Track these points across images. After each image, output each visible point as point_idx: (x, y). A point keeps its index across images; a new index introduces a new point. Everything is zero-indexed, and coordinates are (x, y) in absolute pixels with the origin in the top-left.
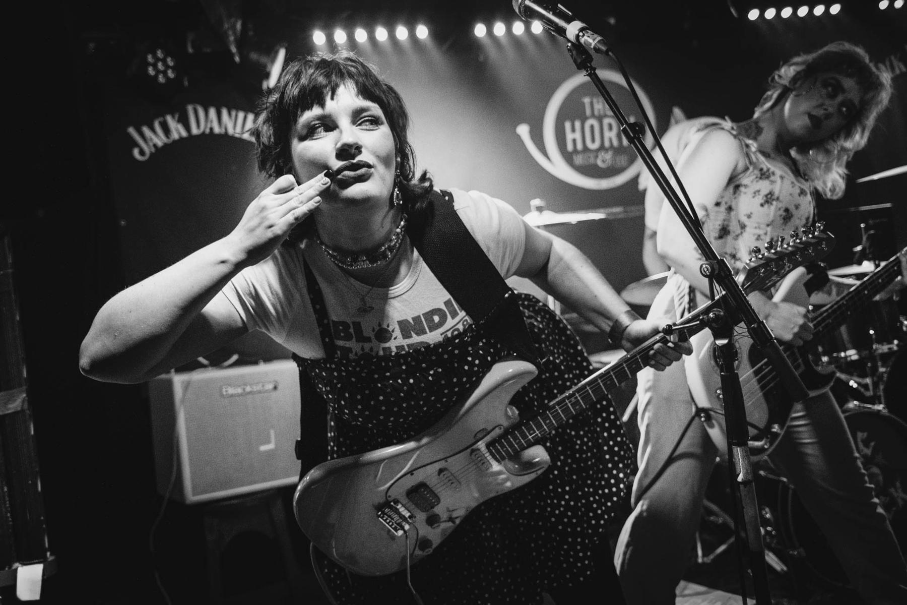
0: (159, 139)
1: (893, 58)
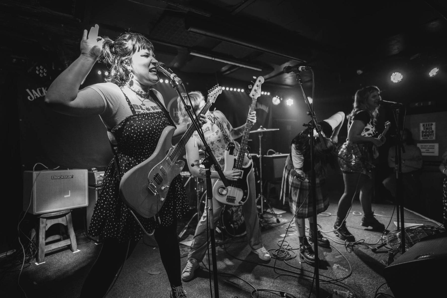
0: (38, 95)
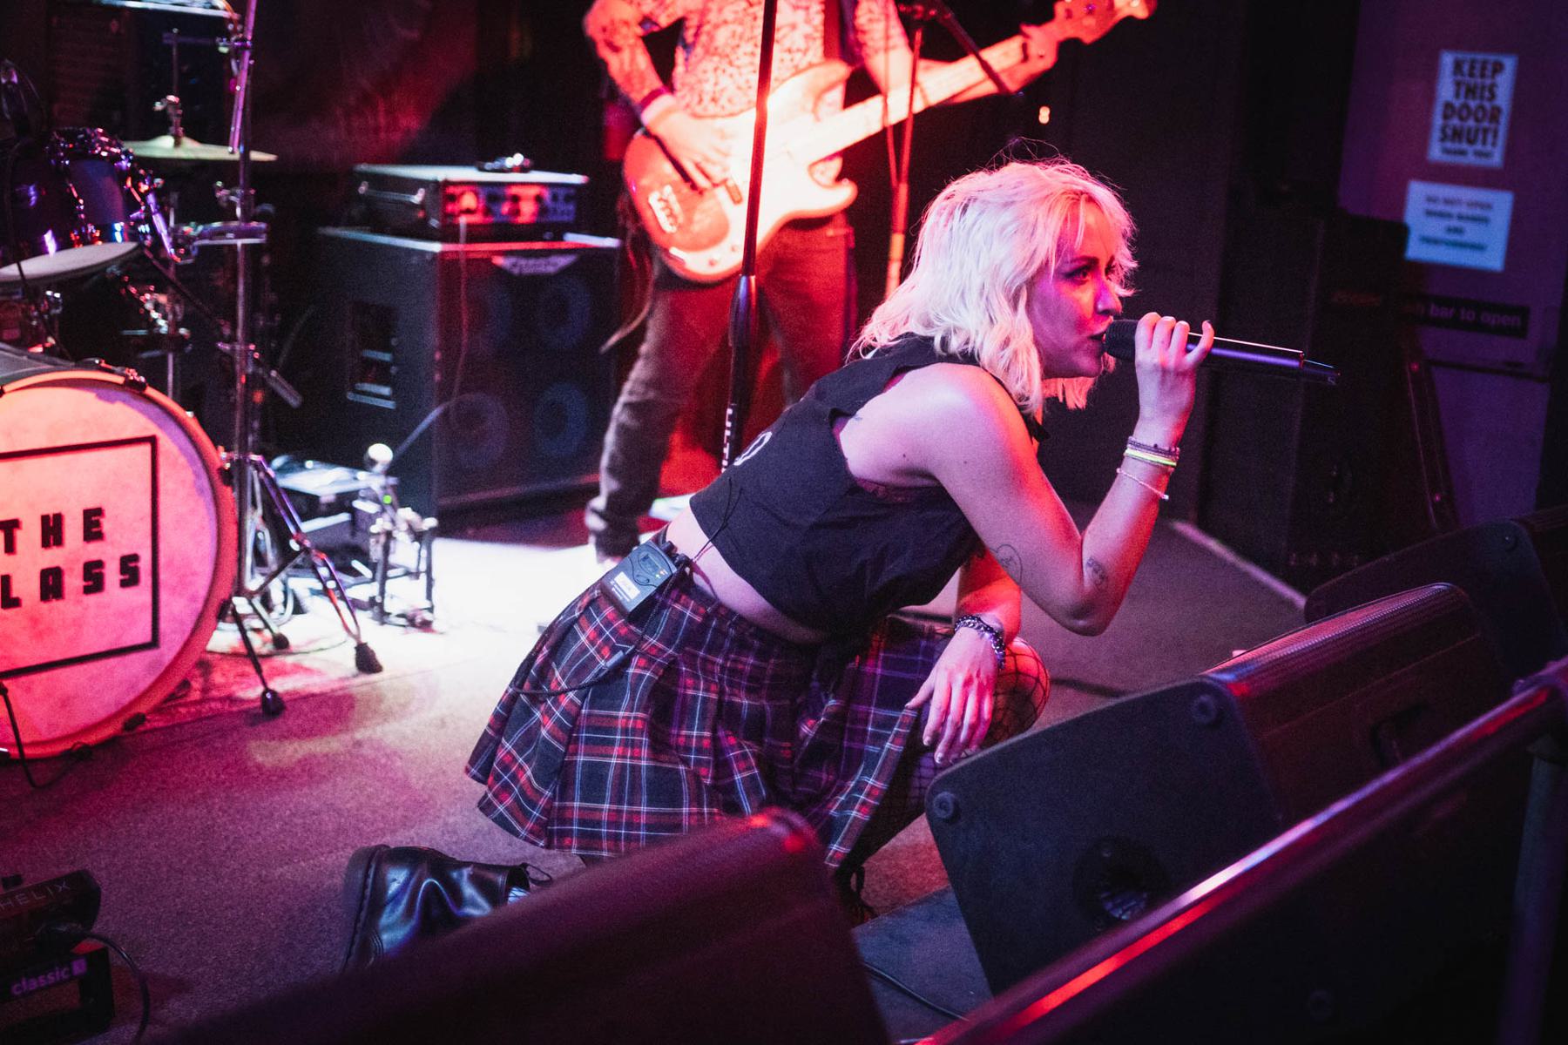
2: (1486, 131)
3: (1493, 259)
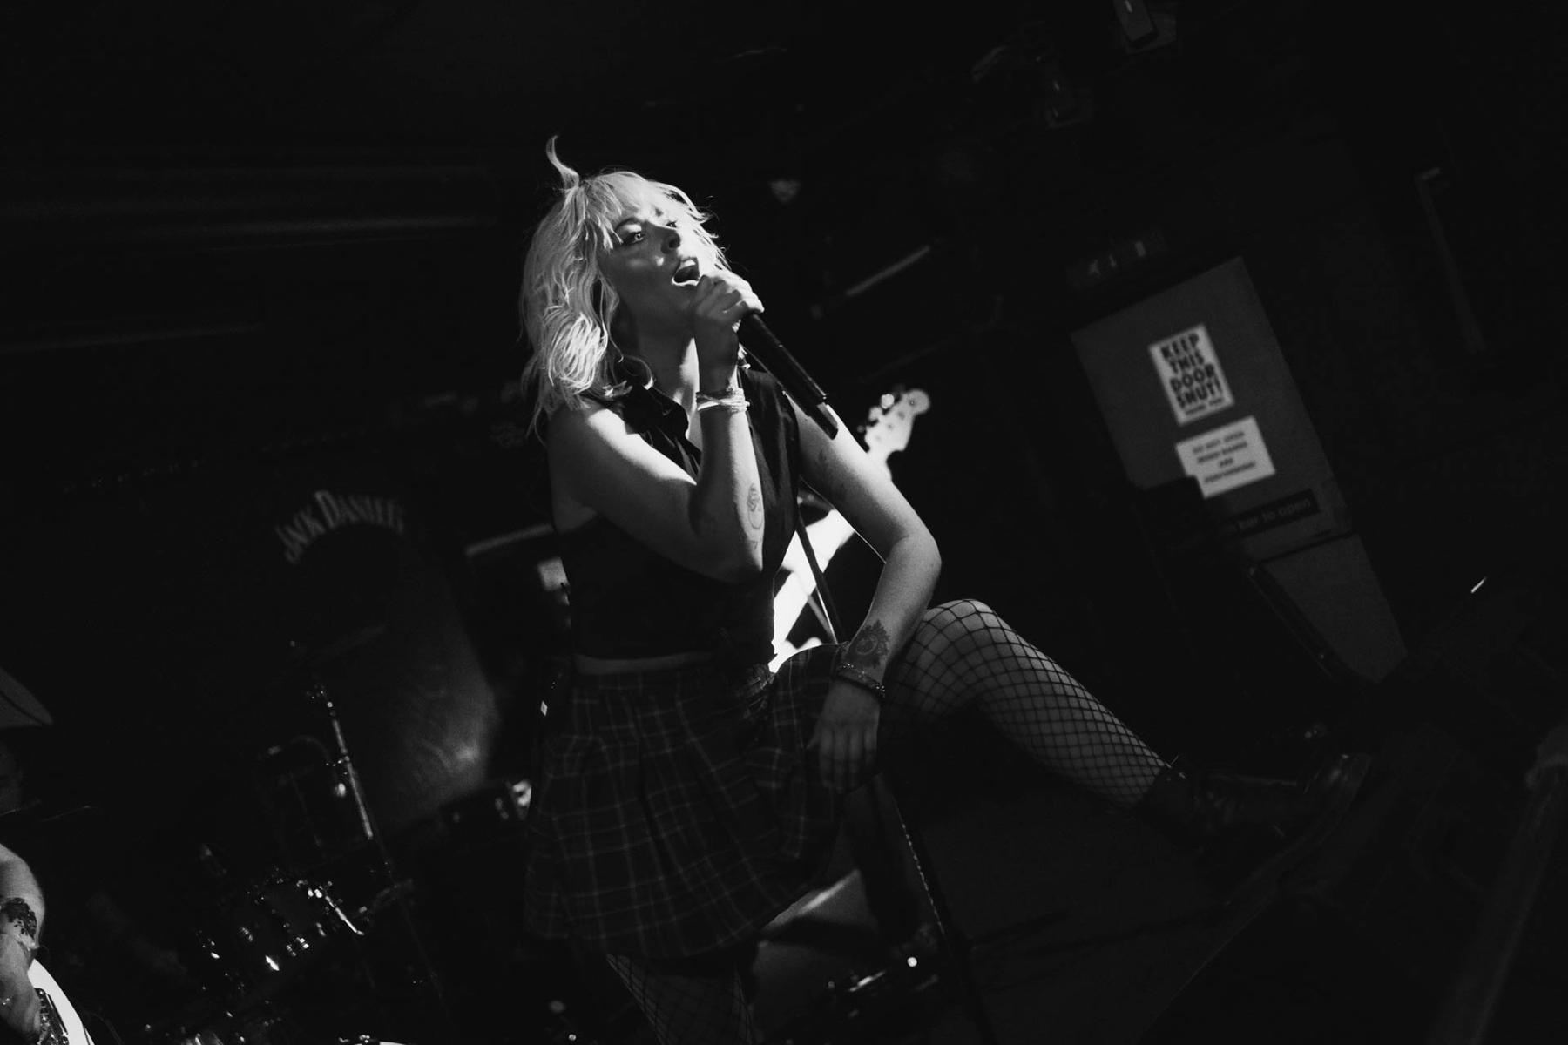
1: (302, 515)
2: (1210, 386)
3: (1264, 467)
